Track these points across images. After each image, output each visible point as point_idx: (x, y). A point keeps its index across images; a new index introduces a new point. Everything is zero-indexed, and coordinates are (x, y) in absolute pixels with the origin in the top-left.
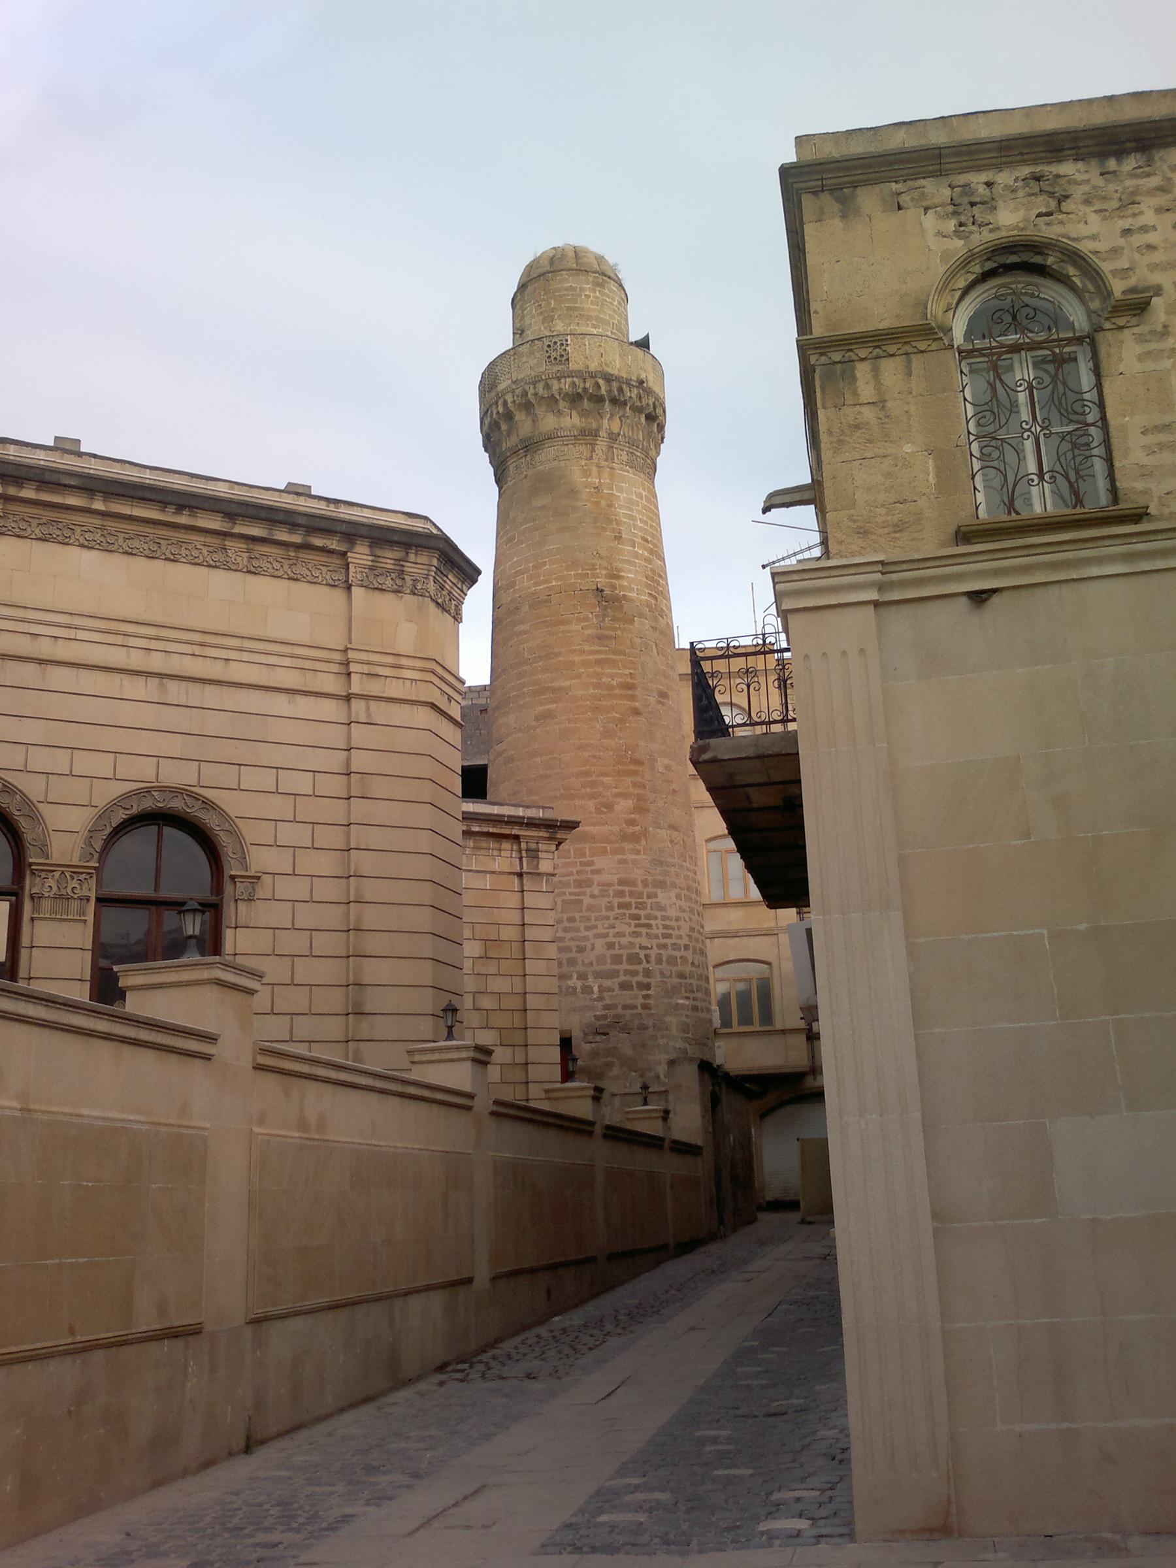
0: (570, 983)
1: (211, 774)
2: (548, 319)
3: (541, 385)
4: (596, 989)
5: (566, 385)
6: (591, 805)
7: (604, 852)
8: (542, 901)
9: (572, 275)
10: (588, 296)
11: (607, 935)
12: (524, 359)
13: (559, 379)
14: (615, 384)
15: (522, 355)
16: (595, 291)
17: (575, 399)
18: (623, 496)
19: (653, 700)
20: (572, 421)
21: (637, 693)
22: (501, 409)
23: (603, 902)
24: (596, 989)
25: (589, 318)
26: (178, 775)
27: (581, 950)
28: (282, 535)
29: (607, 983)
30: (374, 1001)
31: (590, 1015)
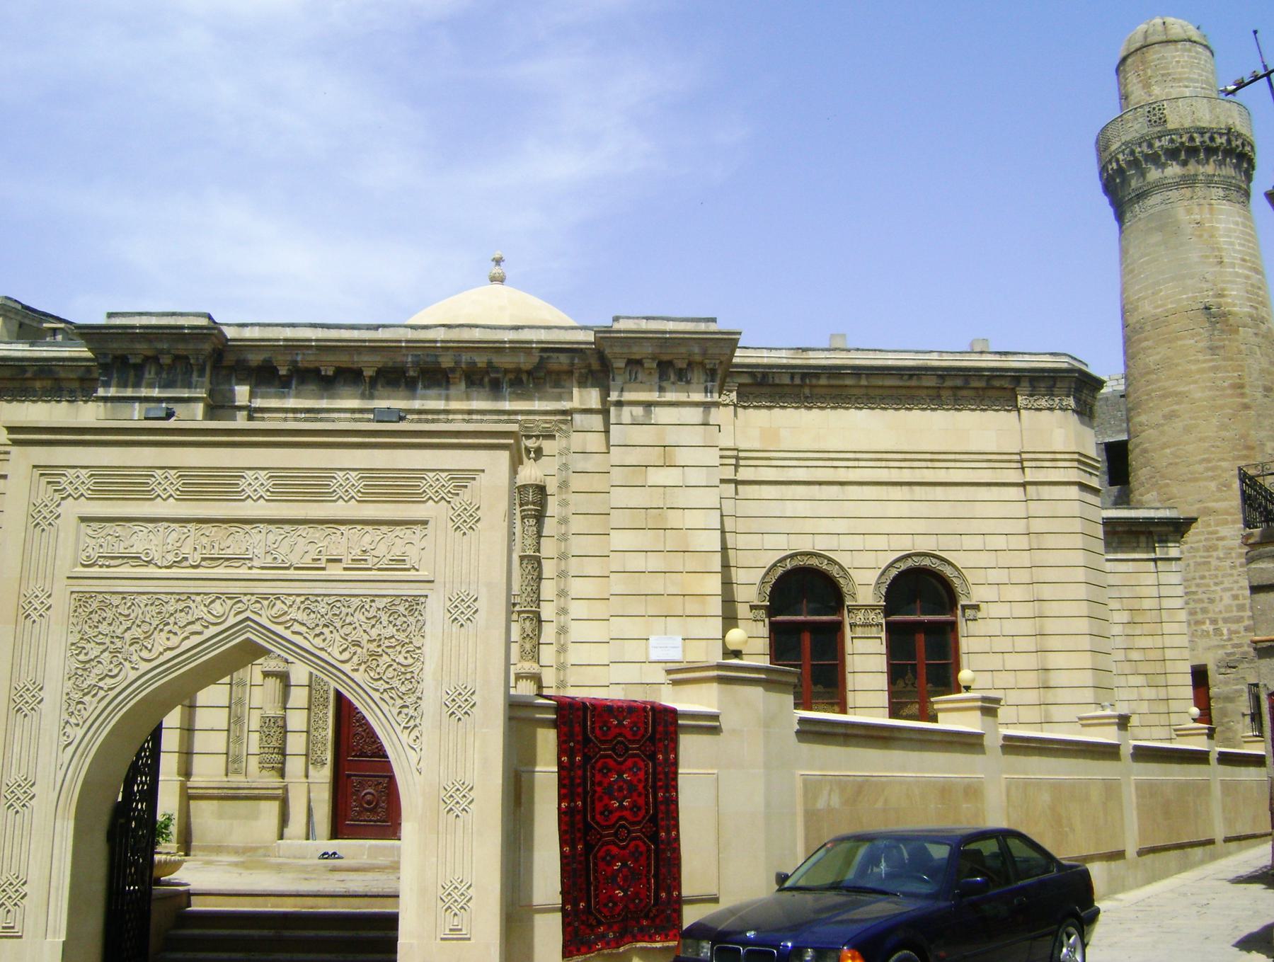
0: (1204, 627)
1: (946, 542)
2: (1147, 85)
3: (1145, 145)
4: (1225, 631)
5: (1165, 141)
6: (1213, 485)
7: (1226, 523)
8: (1175, 579)
10: (1178, 62)
11: (1231, 589)
13: (1159, 138)
14: (1207, 135)
17: (1173, 154)
18: (1221, 226)
19: (1259, 395)
20: (1174, 170)
21: (1247, 390)
22: (1114, 165)
23: (1228, 563)
24: (1225, 631)
25: (1180, 80)
26: (924, 545)
27: (1211, 601)
28: (975, 384)
29: (1234, 627)
30: (1056, 679)
31: (1221, 653)
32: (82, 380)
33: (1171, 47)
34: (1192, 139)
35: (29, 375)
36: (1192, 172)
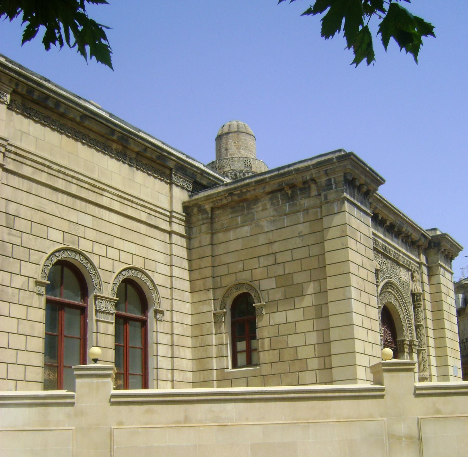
2: (238, 148)
3: (242, 174)
13: (248, 173)
15: (235, 161)
25: (251, 151)
32: (138, 153)
33: (249, 136)
35: (115, 138)
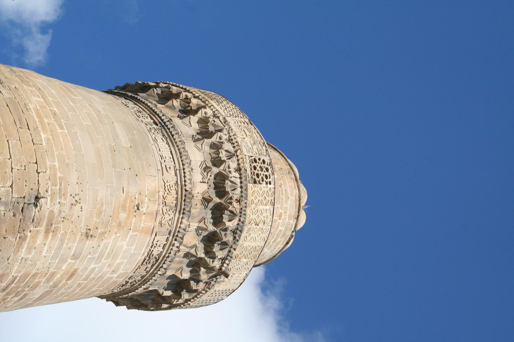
5: (234, 176)
9: (296, 199)
12: (248, 133)
13: (238, 170)
16: (283, 225)
34: (233, 214)
36: (193, 211)
